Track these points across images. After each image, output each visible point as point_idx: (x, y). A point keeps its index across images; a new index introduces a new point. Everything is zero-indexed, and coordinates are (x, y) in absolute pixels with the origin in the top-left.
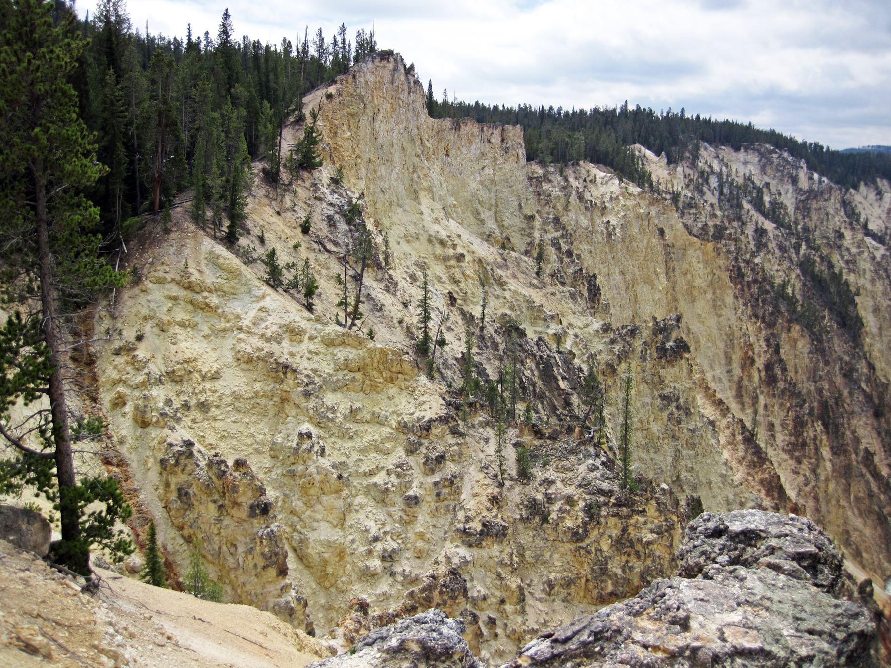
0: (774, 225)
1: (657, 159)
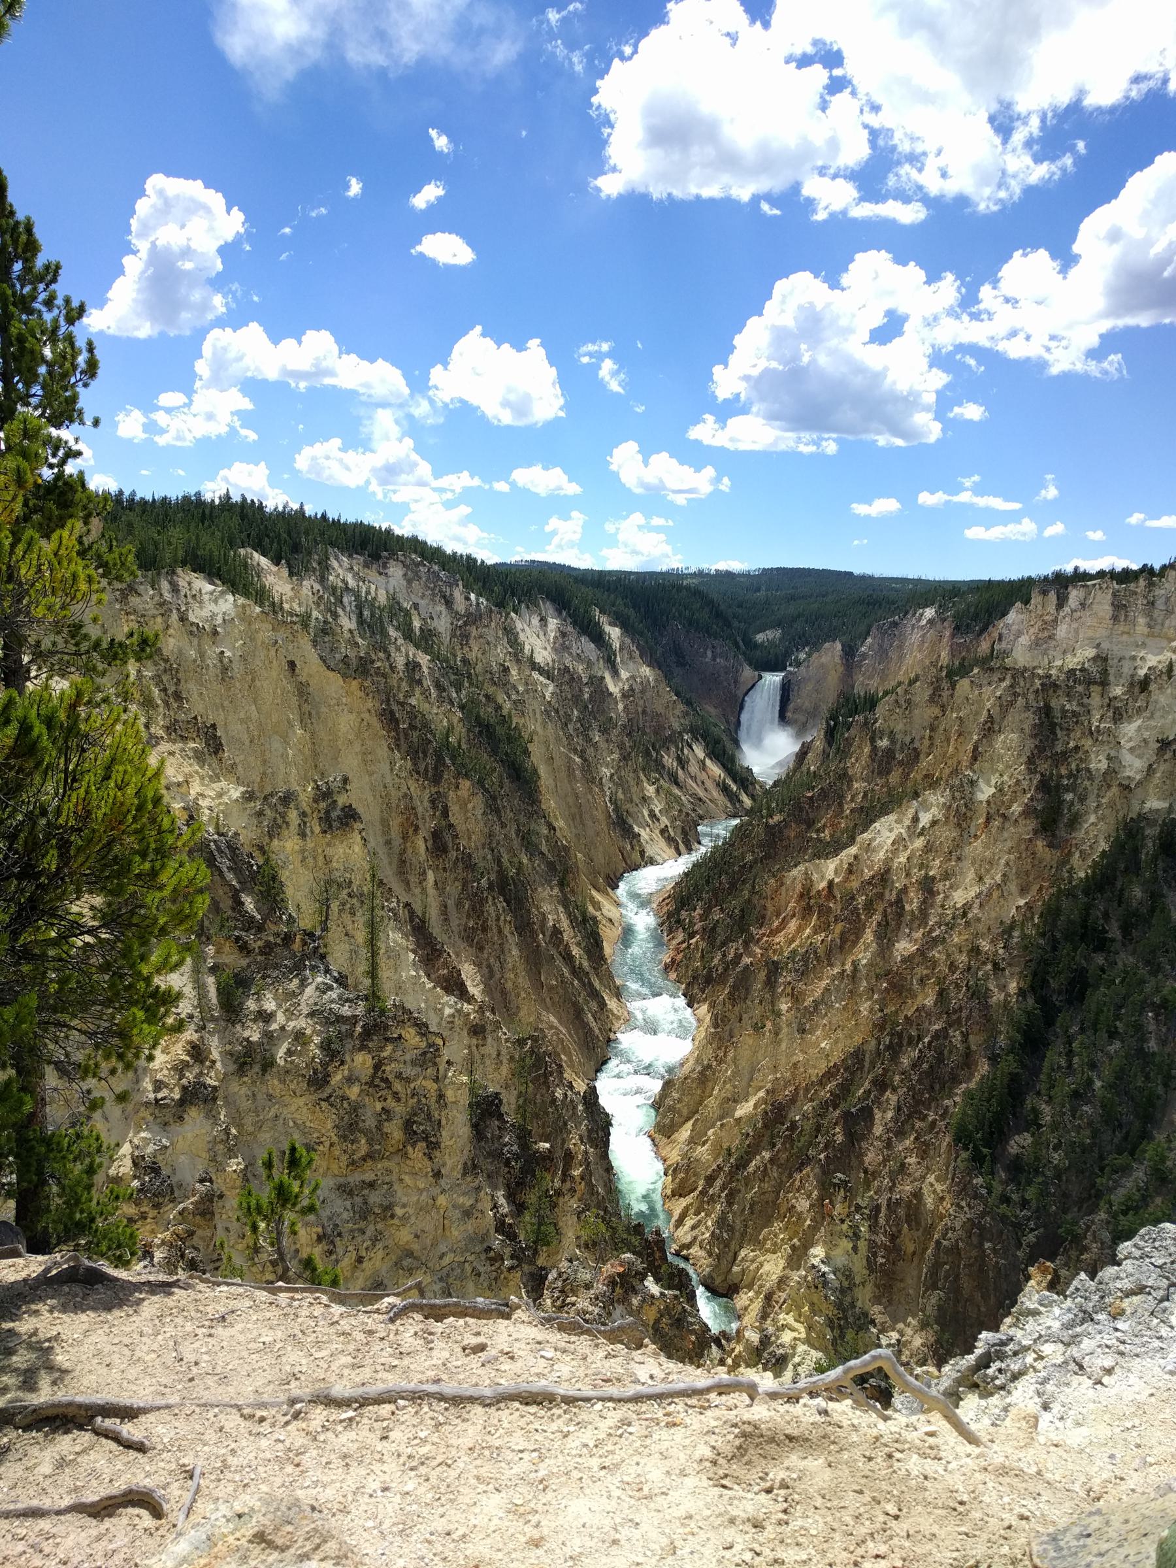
1: (274, 569)
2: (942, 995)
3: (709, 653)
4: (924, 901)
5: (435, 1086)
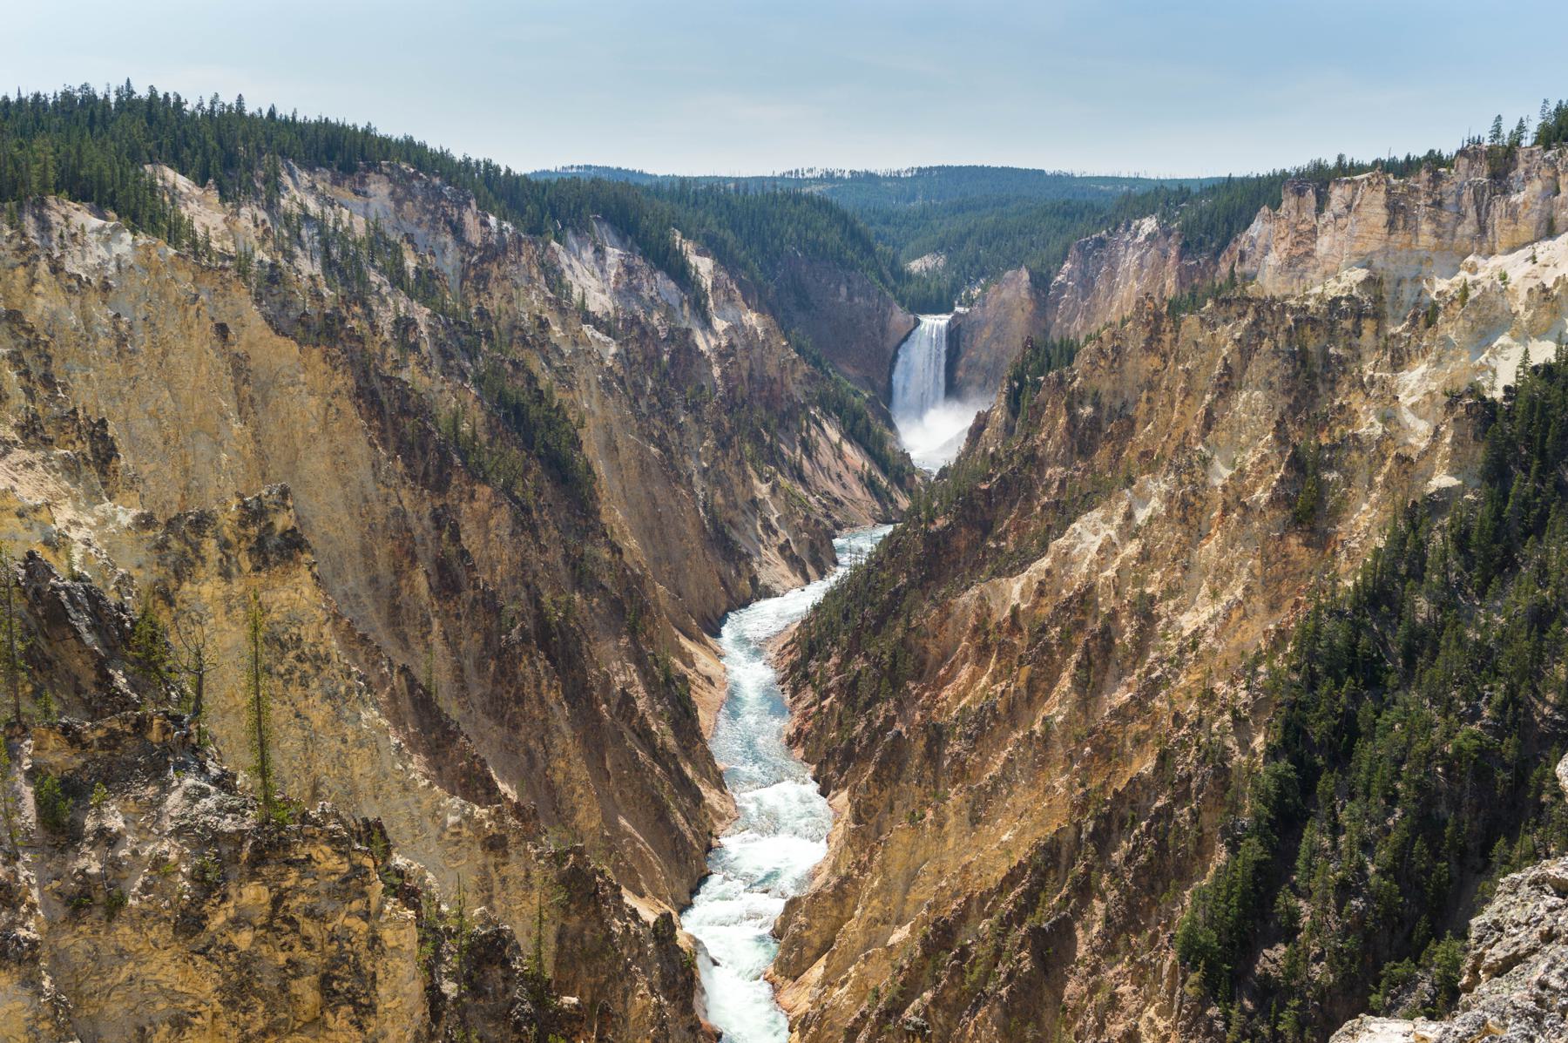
0: (428, 311)
1: (198, 192)
2: (1164, 758)
3: (843, 290)
4: (1140, 630)
5: (365, 926)
